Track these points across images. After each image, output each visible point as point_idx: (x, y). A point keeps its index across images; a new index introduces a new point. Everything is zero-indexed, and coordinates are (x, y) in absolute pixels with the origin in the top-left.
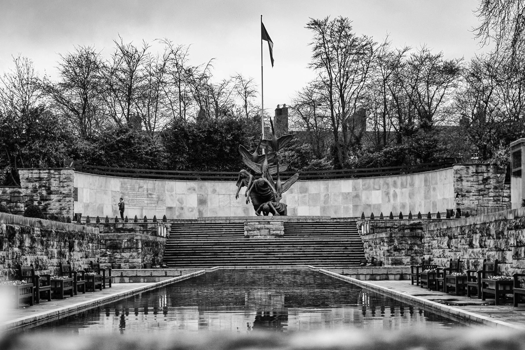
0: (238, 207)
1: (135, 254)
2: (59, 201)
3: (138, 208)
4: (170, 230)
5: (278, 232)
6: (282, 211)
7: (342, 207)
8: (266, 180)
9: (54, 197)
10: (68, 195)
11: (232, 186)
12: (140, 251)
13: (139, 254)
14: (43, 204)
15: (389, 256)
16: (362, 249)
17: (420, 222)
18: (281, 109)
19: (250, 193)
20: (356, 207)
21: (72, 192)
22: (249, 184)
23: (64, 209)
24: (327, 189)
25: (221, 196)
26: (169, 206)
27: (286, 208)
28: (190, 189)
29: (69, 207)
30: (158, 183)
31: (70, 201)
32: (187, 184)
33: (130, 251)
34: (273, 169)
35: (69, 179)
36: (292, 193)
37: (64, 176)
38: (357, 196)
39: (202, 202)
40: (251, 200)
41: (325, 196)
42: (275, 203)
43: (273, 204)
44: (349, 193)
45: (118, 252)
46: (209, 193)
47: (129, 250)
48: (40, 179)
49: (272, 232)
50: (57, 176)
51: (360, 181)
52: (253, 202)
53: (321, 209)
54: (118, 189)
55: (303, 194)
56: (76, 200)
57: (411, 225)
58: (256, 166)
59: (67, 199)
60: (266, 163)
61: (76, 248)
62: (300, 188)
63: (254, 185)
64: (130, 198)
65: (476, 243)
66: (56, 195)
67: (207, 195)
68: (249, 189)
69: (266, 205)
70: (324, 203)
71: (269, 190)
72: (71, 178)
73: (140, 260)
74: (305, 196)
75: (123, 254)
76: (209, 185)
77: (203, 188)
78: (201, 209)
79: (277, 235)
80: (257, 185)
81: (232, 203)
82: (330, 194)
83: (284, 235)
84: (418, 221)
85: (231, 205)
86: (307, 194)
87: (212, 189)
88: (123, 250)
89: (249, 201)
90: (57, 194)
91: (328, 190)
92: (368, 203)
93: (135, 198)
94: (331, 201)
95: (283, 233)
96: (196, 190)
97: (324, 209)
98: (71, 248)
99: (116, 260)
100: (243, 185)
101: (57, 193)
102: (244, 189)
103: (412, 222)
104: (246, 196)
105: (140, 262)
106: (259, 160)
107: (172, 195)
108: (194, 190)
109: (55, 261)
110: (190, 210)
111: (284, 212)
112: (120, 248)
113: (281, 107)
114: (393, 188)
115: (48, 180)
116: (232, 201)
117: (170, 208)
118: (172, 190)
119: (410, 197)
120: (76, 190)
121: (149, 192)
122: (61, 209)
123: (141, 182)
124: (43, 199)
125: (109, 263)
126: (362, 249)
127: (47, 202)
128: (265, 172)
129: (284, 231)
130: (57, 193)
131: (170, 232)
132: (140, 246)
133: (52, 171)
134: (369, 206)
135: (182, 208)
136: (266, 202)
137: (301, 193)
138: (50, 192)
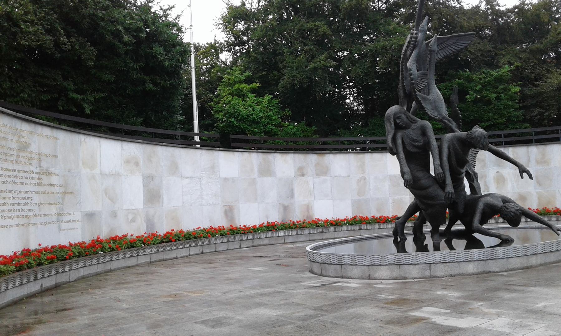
3: (16, 221)
7: (391, 201)
24: (362, 168)
25: (186, 181)
26: (89, 208)
32: (122, 147)
41: (359, 181)
55: (322, 178)
70: (359, 194)
82: (367, 178)
91: (363, 171)
93: (10, 187)
94: (370, 189)
96: (141, 163)
97: (356, 204)
107: (93, 177)
108: (137, 164)
110: (130, 217)
114: (495, 168)
135: (114, 215)
137: (318, 175)
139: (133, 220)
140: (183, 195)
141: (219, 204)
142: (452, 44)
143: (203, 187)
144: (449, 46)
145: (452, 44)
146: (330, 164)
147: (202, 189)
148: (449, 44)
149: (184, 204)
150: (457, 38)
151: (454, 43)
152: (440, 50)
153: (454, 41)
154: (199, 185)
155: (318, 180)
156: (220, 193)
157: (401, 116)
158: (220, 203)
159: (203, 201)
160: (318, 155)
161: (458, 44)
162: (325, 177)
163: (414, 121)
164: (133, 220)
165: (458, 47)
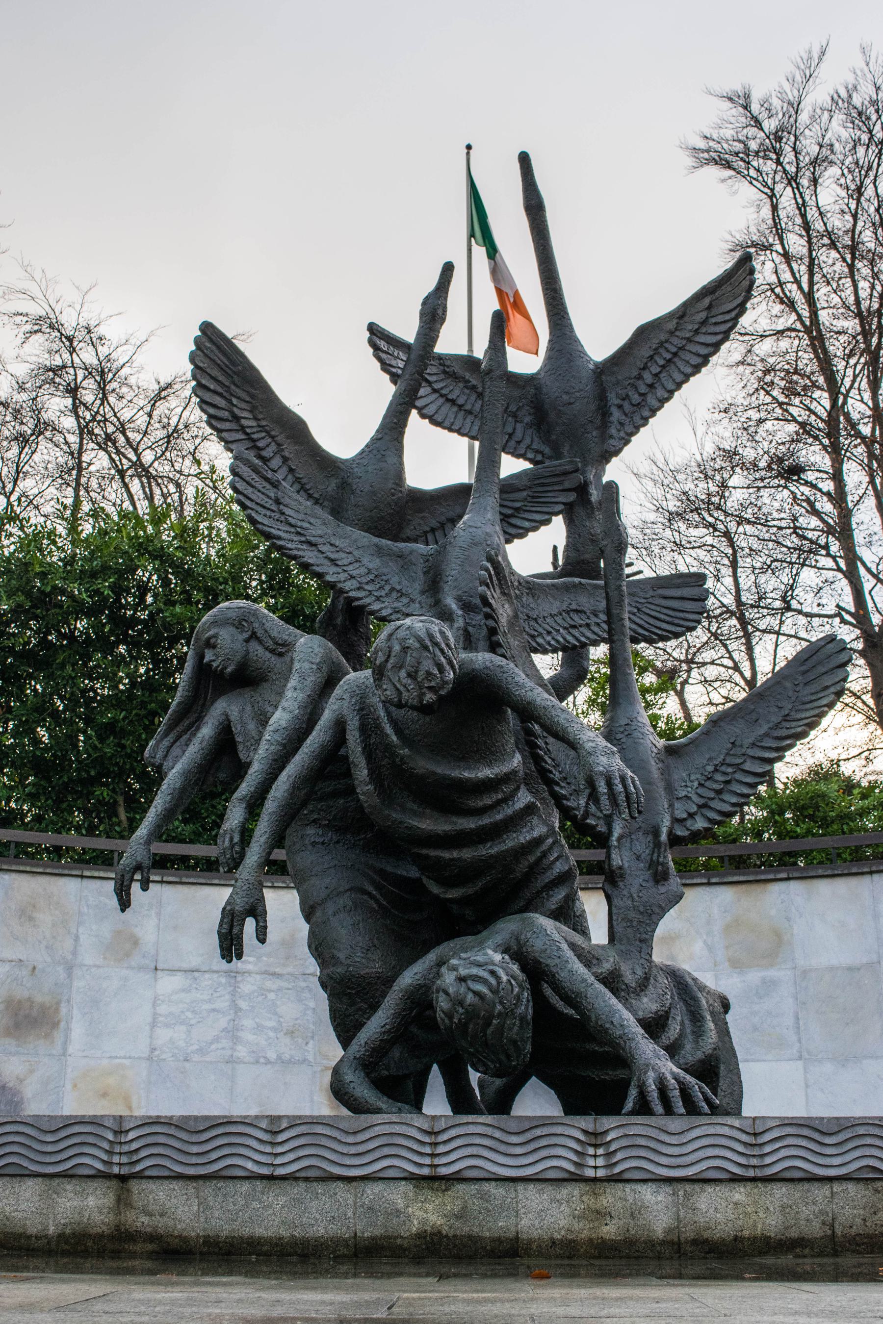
0: (284, 1063)
25: (168, 984)
34: (555, 606)
46: (89, 956)
55: (754, 976)
58: (374, 563)
62: (728, 929)
63: (340, 727)
67: (70, 969)
71: (524, 798)
74: (770, 985)
77: (45, 918)
80: (369, 727)
81: (248, 1036)
85: (242, 1052)
86: (781, 973)
87: (106, 930)
116: (248, 1023)
128: (467, 607)
140: (153, 1025)
141: (305, 1060)
142: (697, 332)
143: (243, 1004)
144: (689, 340)
145: (697, 332)
146: (788, 919)
147: (238, 1009)
148: (688, 335)
149: (157, 1053)
150: (707, 301)
151: (704, 323)
152: (663, 367)
153: (703, 315)
154: (227, 997)
156: (312, 1027)
157: (215, 636)
158: (311, 1058)
159: (239, 1048)
160: (744, 887)
161: (713, 320)
162: (772, 973)
163: (283, 645)
165: (716, 334)
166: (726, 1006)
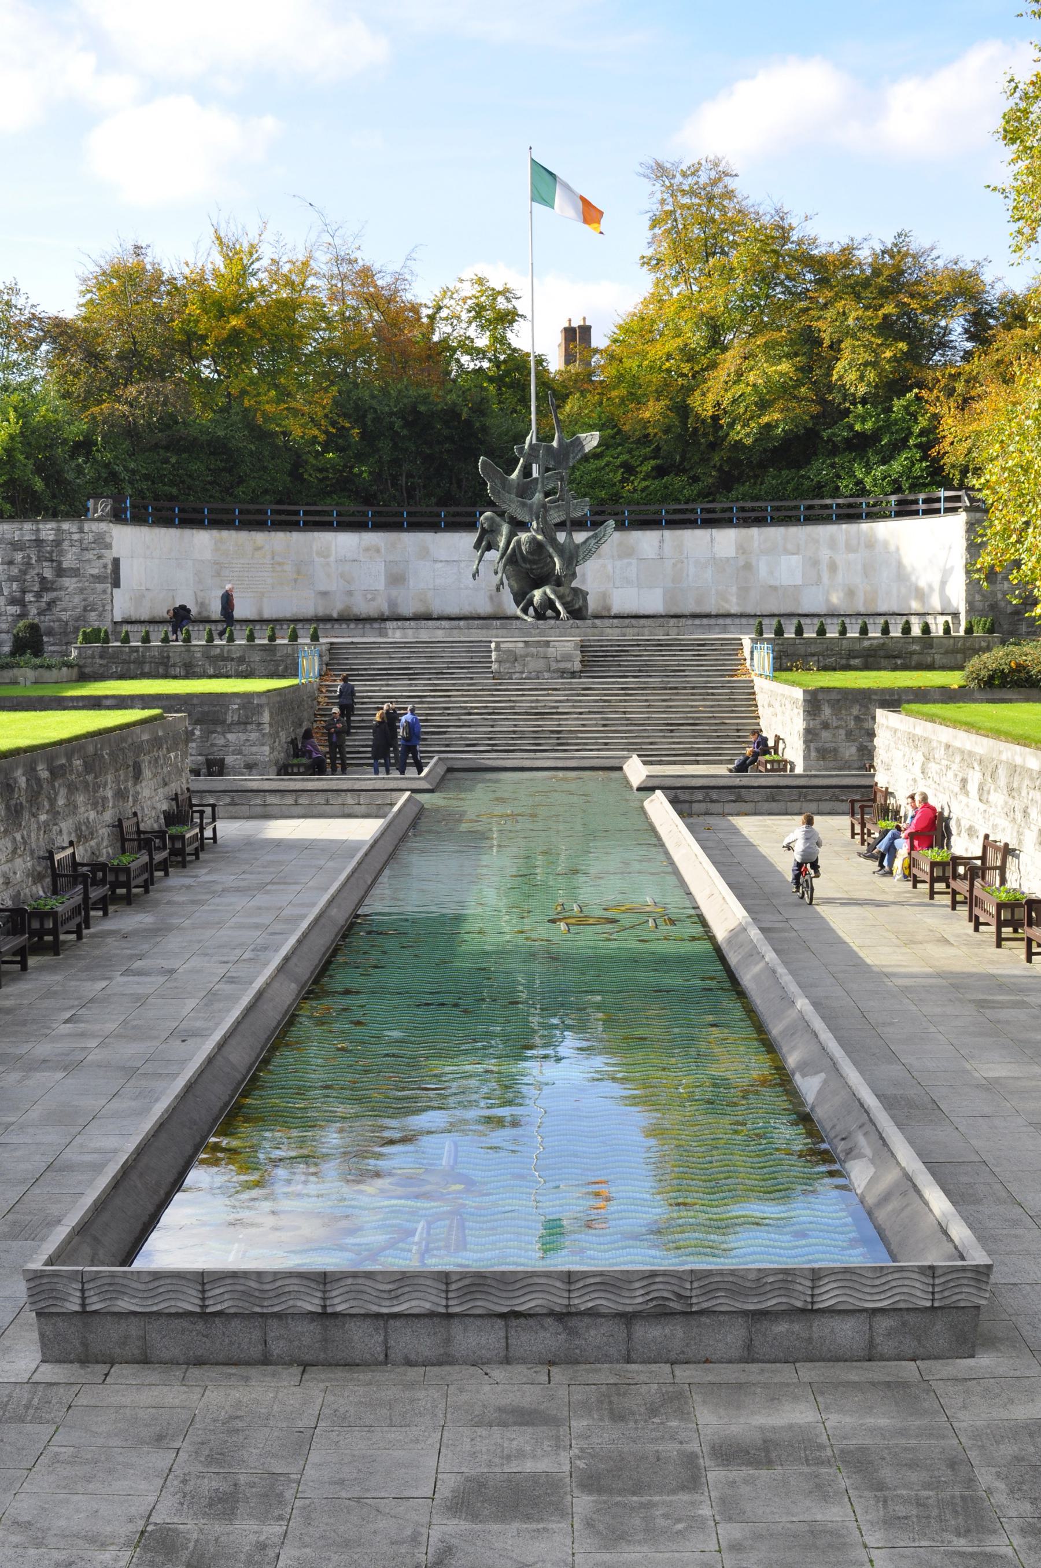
1: (254, 736)
2: (82, 590)
4: (326, 659)
5: (568, 665)
6: (577, 606)
7: (713, 591)
8: (540, 537)
9: (70, 583)
10: (98, 578)
11: (467, 540)
12: (267, 729)
13: (264, 735)
14: (46, 598)
15: (811, 741)
16: (751, 706)
17: (883, 644)
18: (573, 330)
19: (505, 567)
20: (744, 591)
21: (109, 571)
22: (502, 544)
23: (91, 610)
25: (439, 565)
26: (322, 588)
27: (585, 600)
28: (367, 549)
29: (104, 606)
30: (296, 538)
31: (104, 592)
33: (245, 731)
35: (102, 542)
36: (600, 557)
37: (90, 537)
38: (748, 567)
39: (396, 579)
40: (505, 582)
41: (674, 565)
42: (561, 589)
43: (555, 592)
44: (728, 559)
45: (218, 733)
47: (242, 726)
48: (39, 542)
49: (554, 666)
50: (76, 537)
51: (755, 533)
52: (510, 586)
53: (664, 595)
54: (208, 555)
55: (626, 561)
56: (116, 584)
57: (865, 649)
59: (99, 587)
60: (538, 496)
61: (147, 773)
64: (235, 574)
65: (973, 787)
66: (74, 580)
68: (501, 558)
69: (537, 595)
72: (108, 540)
73: (266, 749)
75: (229, 736)
76: (411, 540)
78: (394, 593)
79: (563, 673)
83: (581, 672)
84: (882, 641)
88: (229, 728)
89: (502, 583)
90: (76, 576)
92: (772, 583)
93: (246, 574)
95: (577, 666)
96: (383, 550)
98: (137, 776)
99: (215, 749)
100: (489, 548)
101: (75, 573)
102: (493, 555)
103: (866, 643)
104: (496, 573)
105: (267, 753)
106: (525, 490)
107: (328, 564)
108: (378, 551)
109: (108, 816)
110: (369, 596)
111: (580, 609)
112: (224, 722)
113: (575, 324)
115: (58, 543)
117: (324, 594)
118: (324, 554)
119: (866, 574)
120: (116, 562)
121: (278, 559)
122: (85, 610)
123: (259, 537)
124: (45, 585)
125: (200, 755)
126: (751, 706)
127: (54, 594)
129: (581, 662)
130: (75, 573)
131: (327, 665)
132: (266, 717)
133: (65, 526)
134: (774, 588)
136: (538, 587)
138: (60, 572)
139: (373, 599)
155: (618, 563)
164: (373, 599)
166: (587, 594)
